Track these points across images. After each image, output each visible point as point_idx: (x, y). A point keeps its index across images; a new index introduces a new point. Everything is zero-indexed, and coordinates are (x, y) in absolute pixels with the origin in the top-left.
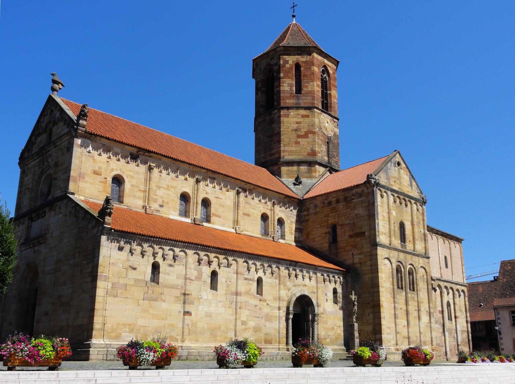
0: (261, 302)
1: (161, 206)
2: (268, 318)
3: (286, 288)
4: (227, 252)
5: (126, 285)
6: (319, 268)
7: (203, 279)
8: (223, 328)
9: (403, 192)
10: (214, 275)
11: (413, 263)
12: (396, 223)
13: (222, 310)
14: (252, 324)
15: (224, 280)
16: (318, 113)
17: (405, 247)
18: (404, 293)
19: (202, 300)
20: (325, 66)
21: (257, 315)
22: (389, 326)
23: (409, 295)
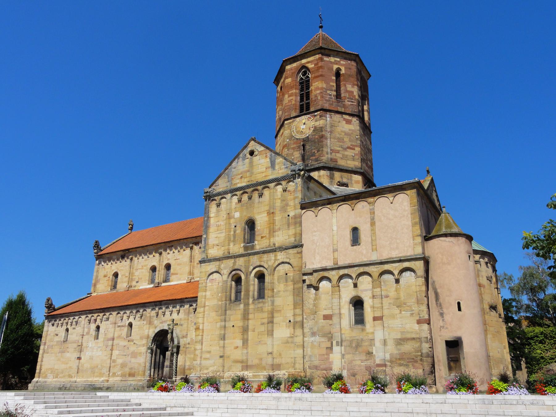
0: (130, 343)
1: (137, 282)
2: (134, 355)
3: (153, 326)
4: (104, 310)
5: (52, 346)
6: (185, 300)
7: (90, 334)
8: (99, 366)
9: (255, 182)
10: (98, 328)
11: (262, 264)
12: (237, 226)
13: (100, 353)
14: (120, 361)
15: (103, 330)
16: (290, 123)
17: (253, 247)
18: (242, 306)
19: (88, 348)
20: (304, 67)
21: (125, 354)
22: (209, 350)
23: (251, 307)
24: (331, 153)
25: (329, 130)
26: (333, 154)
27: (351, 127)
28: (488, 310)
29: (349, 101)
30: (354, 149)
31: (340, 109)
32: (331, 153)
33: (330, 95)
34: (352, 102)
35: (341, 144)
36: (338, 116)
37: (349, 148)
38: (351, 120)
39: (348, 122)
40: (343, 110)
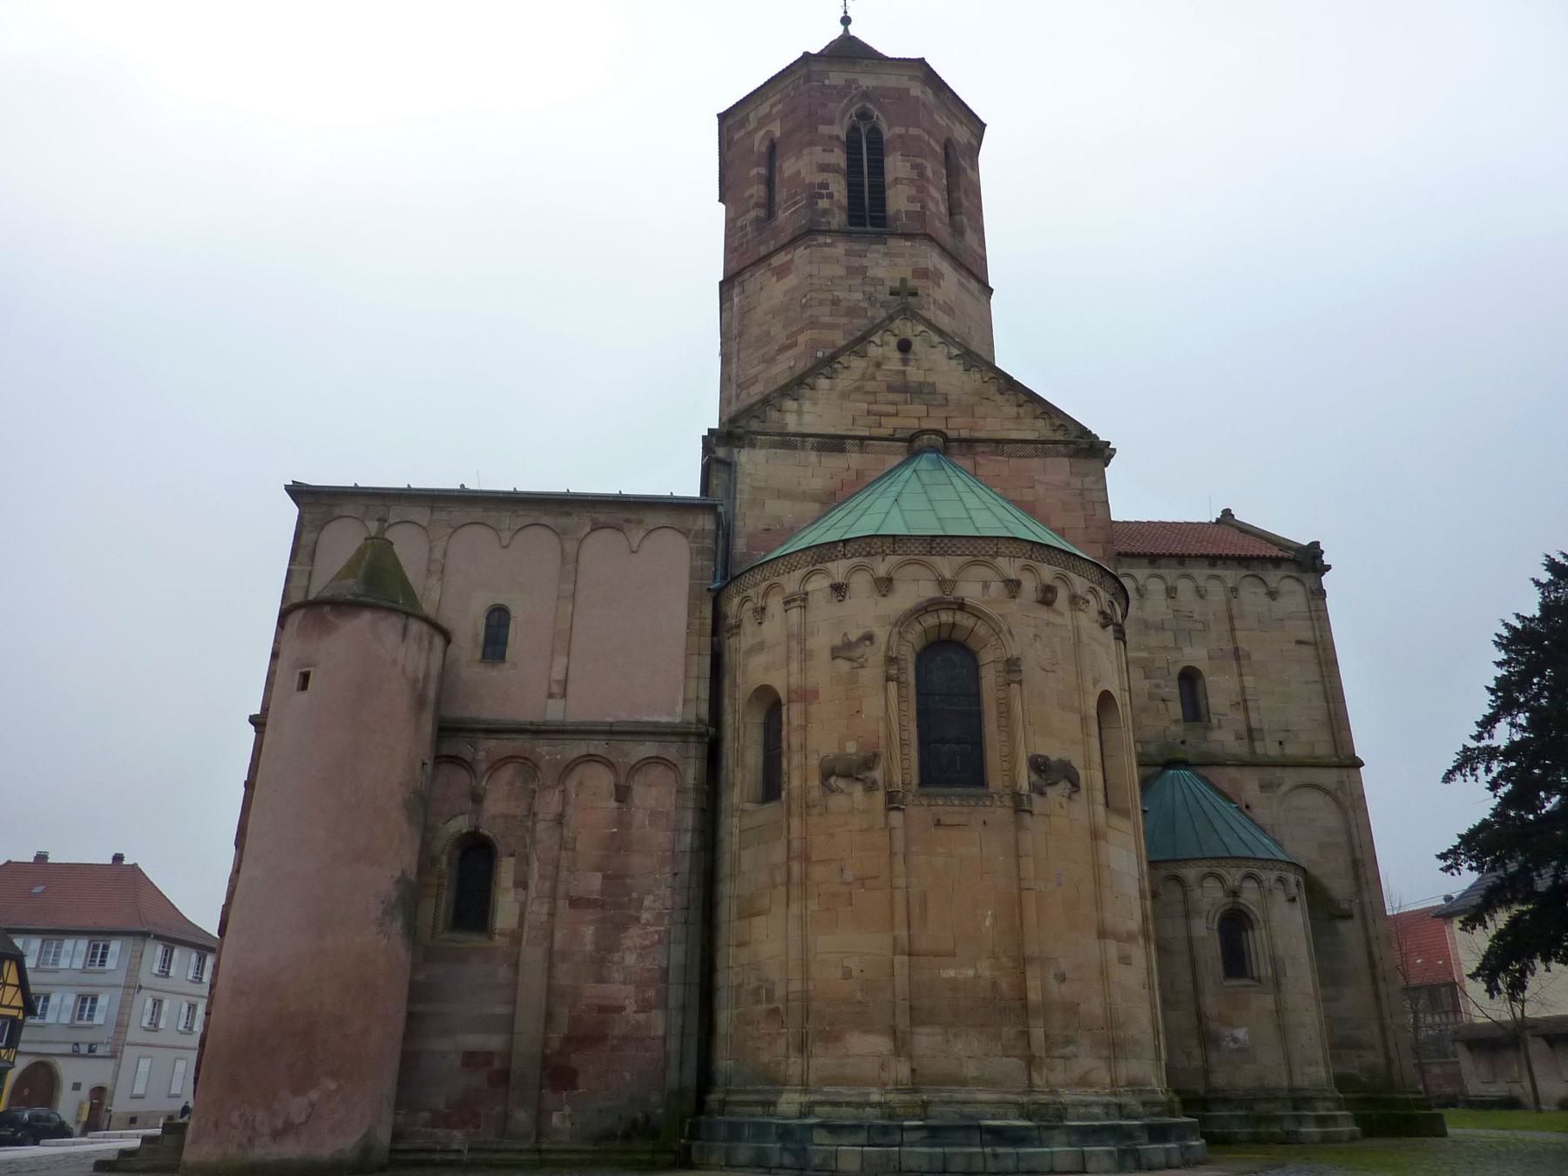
24: (738, 396)
25: (735, 332)
26: (744, 393)
27: (791, 280)
28: (816, 793)
29: (787, 208)
30: (795, 344)
31: (763, 250)
32: (738, 396)
33: (743, 228)
34: (795, 203)
35: (761, 352)
36: (760, 273)
37: (784, 348)
38: (792, 261)
39: (782, 272)
40: (772, 245)
